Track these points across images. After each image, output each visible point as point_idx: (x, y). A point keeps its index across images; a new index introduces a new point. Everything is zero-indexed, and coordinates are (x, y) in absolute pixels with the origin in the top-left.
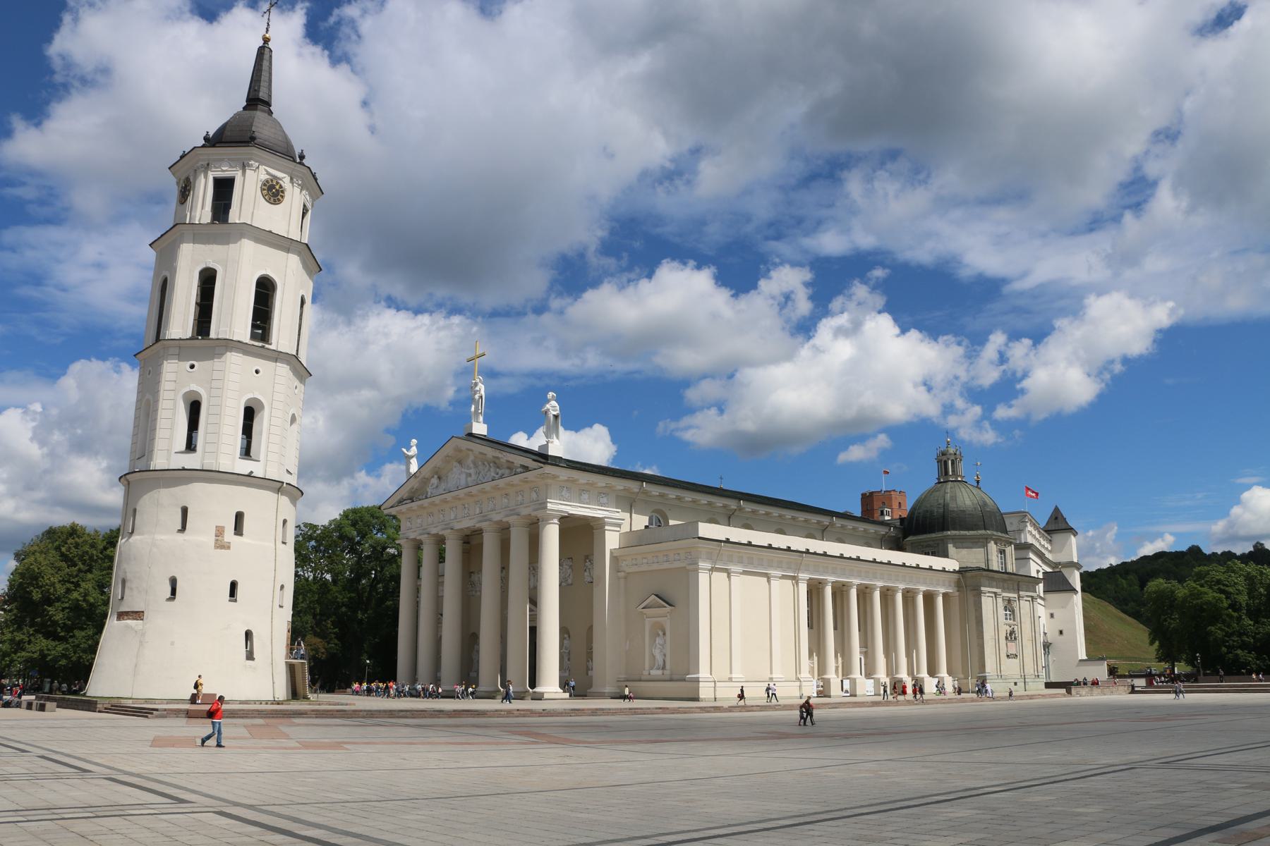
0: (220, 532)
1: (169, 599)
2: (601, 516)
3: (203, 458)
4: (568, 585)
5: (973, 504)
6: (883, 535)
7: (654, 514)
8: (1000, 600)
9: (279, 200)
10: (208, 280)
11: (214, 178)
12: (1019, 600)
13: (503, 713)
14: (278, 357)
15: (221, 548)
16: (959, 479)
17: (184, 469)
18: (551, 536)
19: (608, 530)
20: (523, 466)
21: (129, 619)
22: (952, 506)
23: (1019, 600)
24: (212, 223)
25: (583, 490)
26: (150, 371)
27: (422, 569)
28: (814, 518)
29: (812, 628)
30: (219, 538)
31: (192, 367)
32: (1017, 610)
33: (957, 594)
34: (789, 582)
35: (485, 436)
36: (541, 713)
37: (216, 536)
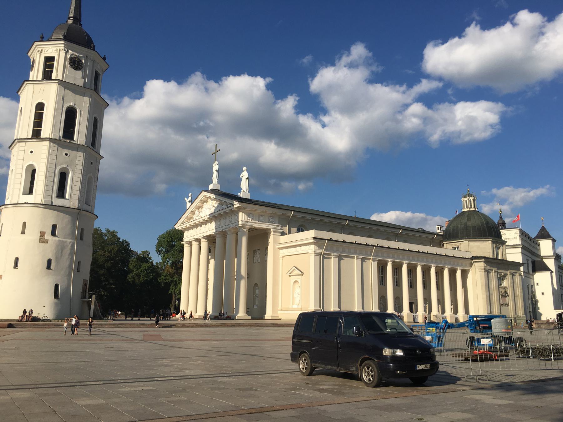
0: (42, 234)
1: (15, 268)
4: (259, 262)
5: (481, 222)
6: (430, 239)
7: (301, 227)
9: (80, 68)
13: (180, 325)
14: (77, 148)
15: (43, 243)
22: (469, 224)
24: (42, 80)
25: (261, 215)
27: (200, 256)
28: (390, 230)
29: (426, 289)
30: (43, 238)
31: (31, 152)
35: (219, 190)
36: (202, 325)
37: (40, 237)
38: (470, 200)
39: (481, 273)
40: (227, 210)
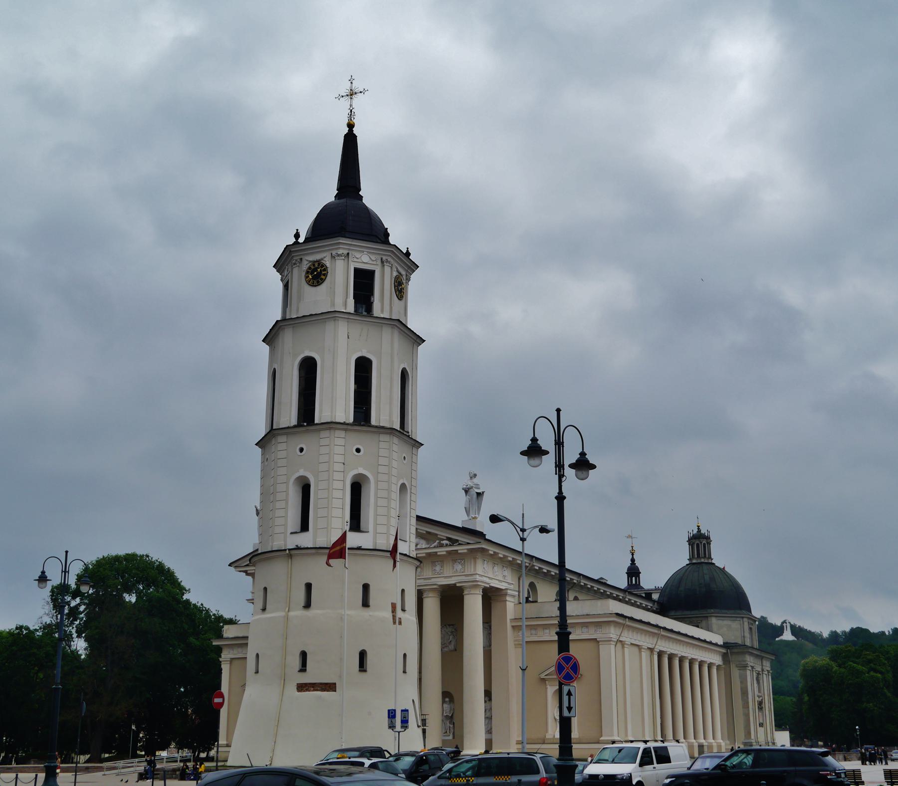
0: (394, 606)
2: (503, 588)
3: (375, 538)
8: (754, 673)
10: (363, 368)
11: (354, 268)
12: (763, 673)
16: (710, 561)
17: (359, 548)
18: (473, 606)
19: (509, 601)
20: (449, 539)
21: (317, 690)
23: (763, 673)
26: (301, 450)
31: (358, 450)
32: (761, 681)
33: (724, 666)
34: (648, 652)
38: (704, 544)
39: (741, 671)
40: (442, 551)
